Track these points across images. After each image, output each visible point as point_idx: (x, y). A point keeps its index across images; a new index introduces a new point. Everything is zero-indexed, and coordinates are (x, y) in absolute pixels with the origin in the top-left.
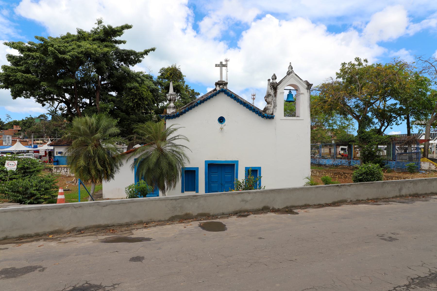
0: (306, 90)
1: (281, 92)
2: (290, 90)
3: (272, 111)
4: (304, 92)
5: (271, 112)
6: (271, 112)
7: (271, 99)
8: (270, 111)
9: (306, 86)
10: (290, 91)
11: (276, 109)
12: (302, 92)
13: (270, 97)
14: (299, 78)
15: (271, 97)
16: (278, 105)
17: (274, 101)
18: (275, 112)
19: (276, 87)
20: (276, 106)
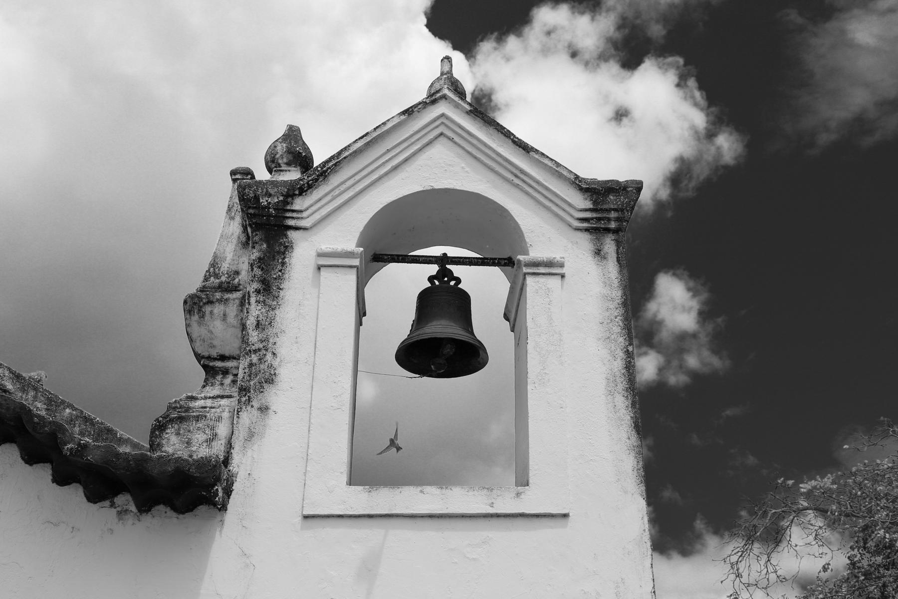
0: (585, 242)
1: (326, 247)
2: (443, 260)
3: (223, 430)
4: (557, 256)
5: (210, 441)
6: (210, 441)
7: (232, 318)
8: (199, 437)
9: (580, 201)
10: (444, 274)
11: (264, 409)
12: (536, 253)
13: (218, 309)
14: (507, 134)
15: (232, 310)
16: (286, 374)
17: (254, 336)
18: (251, 435)
19: (283, 208)
20: (270, 380)
